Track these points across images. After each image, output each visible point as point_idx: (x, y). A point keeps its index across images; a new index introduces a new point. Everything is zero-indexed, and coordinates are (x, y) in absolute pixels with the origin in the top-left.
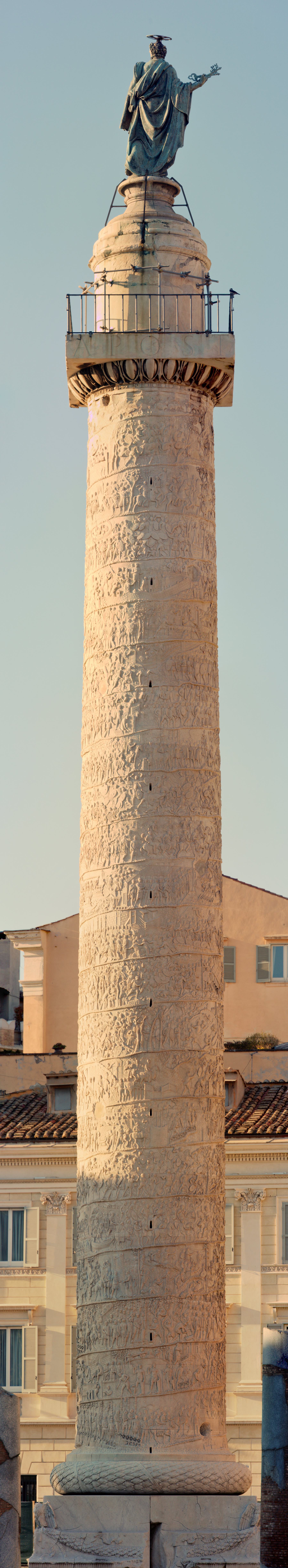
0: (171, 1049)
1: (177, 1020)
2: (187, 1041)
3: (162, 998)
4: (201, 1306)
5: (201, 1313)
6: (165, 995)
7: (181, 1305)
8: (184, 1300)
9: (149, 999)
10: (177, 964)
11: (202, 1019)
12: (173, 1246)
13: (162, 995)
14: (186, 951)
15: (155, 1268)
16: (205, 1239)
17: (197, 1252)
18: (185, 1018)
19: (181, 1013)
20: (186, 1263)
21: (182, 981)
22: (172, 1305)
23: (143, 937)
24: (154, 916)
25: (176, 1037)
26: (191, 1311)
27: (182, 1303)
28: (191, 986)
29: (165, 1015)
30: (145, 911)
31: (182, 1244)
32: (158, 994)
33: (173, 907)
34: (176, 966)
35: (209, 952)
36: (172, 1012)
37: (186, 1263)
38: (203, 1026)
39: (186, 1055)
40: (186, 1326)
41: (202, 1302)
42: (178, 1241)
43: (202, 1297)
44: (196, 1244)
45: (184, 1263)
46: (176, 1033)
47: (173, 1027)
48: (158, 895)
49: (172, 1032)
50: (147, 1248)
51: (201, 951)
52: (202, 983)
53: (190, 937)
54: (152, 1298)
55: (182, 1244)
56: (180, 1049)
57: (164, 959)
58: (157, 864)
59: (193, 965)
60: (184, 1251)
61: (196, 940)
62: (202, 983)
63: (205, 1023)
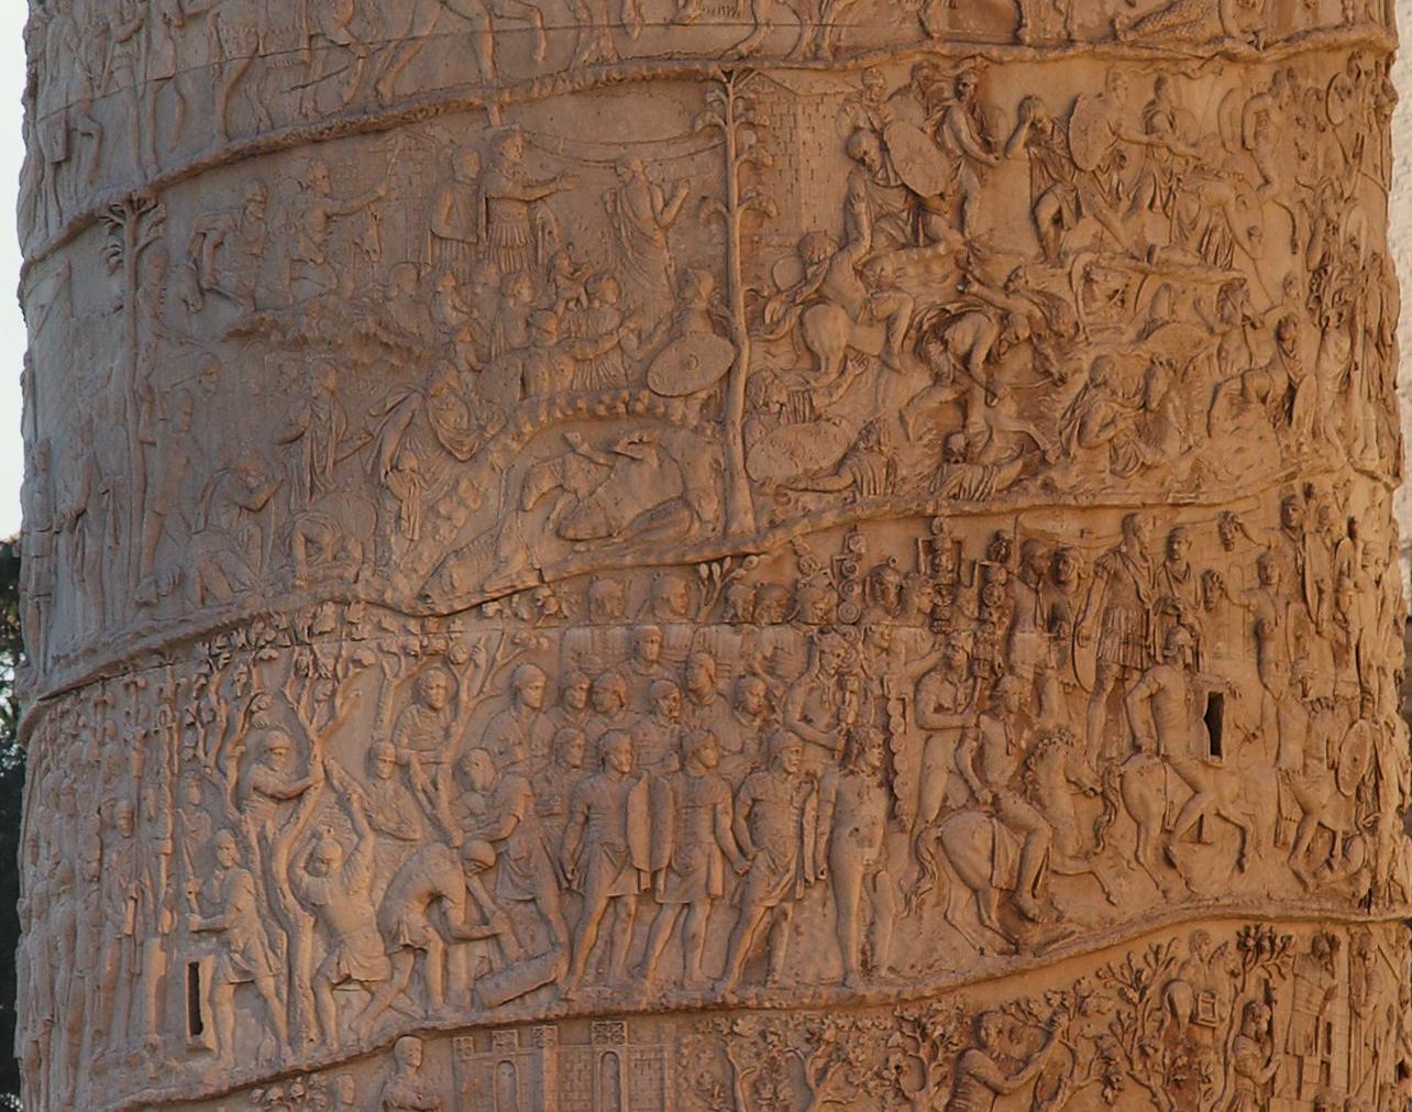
4: (664, 677)
5: (657, 736)
7: (438, 678)
8: (468, 632)
12: (363, 132)
15: (227, 353)
16: (724, 36)
17: (613, 165)
20: (491, 273)
22: (364, 685)
26: (544, 727)
27: (448, 661)
31: (447, 106)
37: (491, 273)
40: (483, 870)
41: (681, 632)
42: (407, 86)
43: (675, 587)
44: (603, 87)
45: (464, 283)
50: (175, 181)
54: (206, 636)
55: (447, 106)
60: (471, 170)
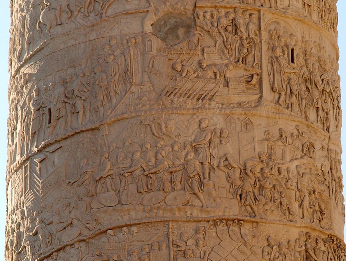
14: (125, 219)
23: (38, 214)
24: (56, 160)
30: (42, 156)
33: (92, 129)
35: (196, 213)
48: (63, 112)
51: (169, 214)
53: (133, 188)
57: (72, 251)
58: (62, 46)
61: (149, 190)
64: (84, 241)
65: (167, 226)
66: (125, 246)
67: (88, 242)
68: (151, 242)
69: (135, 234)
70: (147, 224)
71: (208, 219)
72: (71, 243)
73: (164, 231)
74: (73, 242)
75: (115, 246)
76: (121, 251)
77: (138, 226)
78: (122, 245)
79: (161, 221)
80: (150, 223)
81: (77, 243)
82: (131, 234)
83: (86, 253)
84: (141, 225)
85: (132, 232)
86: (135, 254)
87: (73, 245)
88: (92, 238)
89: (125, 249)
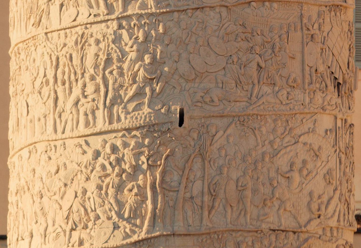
0: (230, 226)
1: (244, 160)
2: (267, 210)
3: (208, 107)
6: (216, 99)
9: (176, 108)
10: (243, 25)
11: (303, 155)
13: (208, 100)
18: (264, 154)
19: (252, 141)
21: (255, 67)
25: (241, 199)
28: (277, 78)
29: (216, 146)
32: (198, 97)
34: (241, 29)
36: (231, 139)
38: (305, 172)
39: (266, 242)
46: (241, 189)
47: (234, 176)
49: (232, 186)
52: (303, 70)
56: (252, 228)
57: (212, 13)
59: (281, 28)
62: (303, 70)
63: (310, 166)
64: (227, 7)
65: (300, 8)
66: (267, 21)
67: (230, 9)
68: (288, 22)
69: (275, 11)
70: (286, 3)
71: (327, 4)
72: (212, 5)
73: (298, 12)
74: (215, 5)
75: (259, 20)
76: (263, 27)
77: (278, 3)
78: (265, 20)
79: (298, 2)
80: (288, 3)
81: (218, 7)
82: (271, 10)
83: (227, 19)
84: (281, 3)
85: (273, 8)
86: (276, 32)
87: (213, 7)
88: (234, 6)
89: (267, 25)
